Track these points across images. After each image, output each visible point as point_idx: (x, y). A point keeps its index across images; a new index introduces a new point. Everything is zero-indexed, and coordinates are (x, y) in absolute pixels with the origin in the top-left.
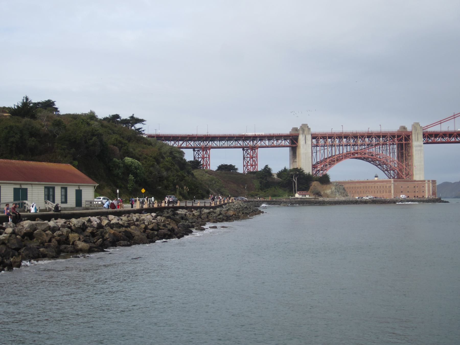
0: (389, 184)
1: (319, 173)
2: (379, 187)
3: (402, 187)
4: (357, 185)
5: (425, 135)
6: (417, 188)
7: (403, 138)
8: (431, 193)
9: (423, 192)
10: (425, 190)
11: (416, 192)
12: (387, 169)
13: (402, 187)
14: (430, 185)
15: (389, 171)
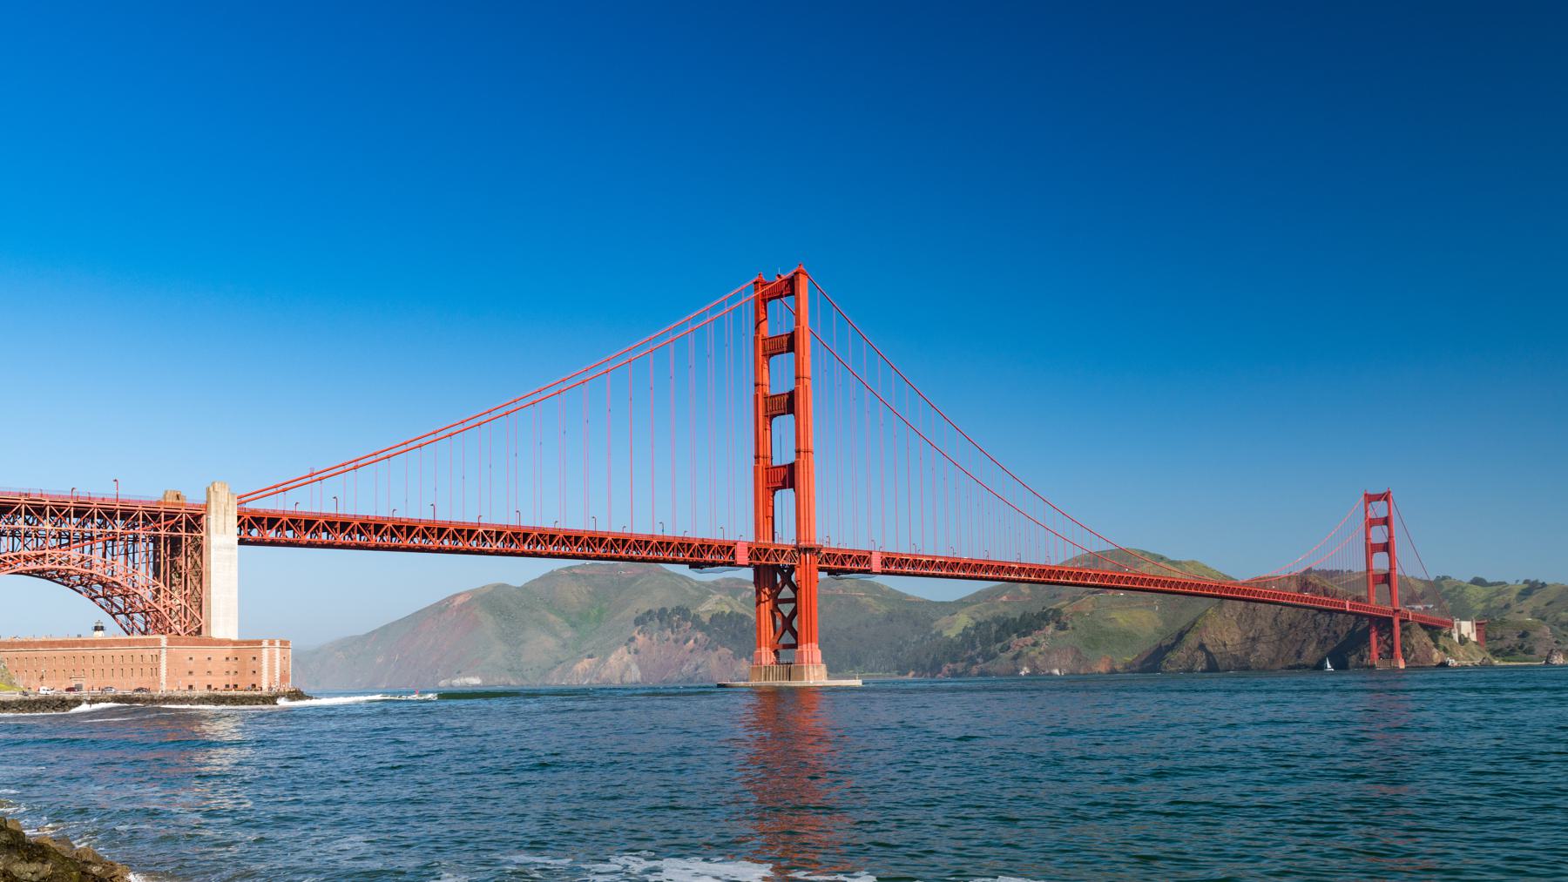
5: (243, 519)
7: (181, 522)
8: (278, 676)
9: (254, 672)
10: (261, 669)
11: (232, 673)
13: (191, 659)
14: (274, 655)
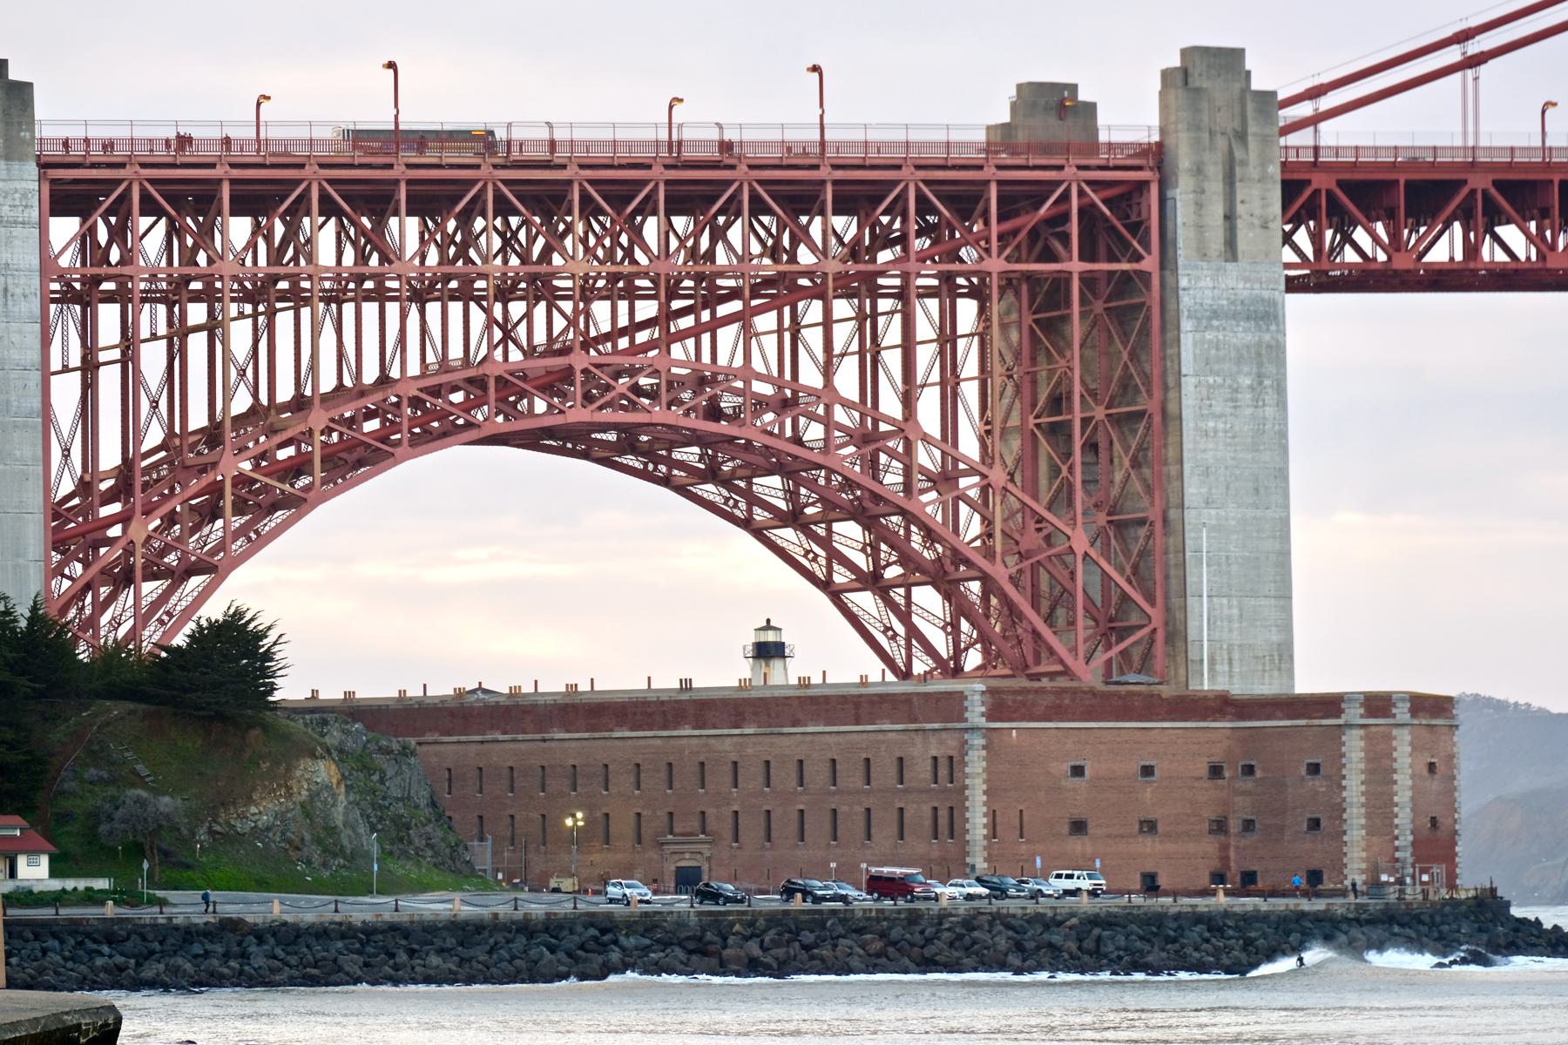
0: (933, 739)
1: (112, 598)
2: (817, 774)
3: (1078, 771)
4: (568, 744)
6: (1248, 784)
7: (1065, 218)
9: (1315, 824)
10: (1339, 810)
12: (878, 570)
13: (1078, 771)
15: (898, 595)
